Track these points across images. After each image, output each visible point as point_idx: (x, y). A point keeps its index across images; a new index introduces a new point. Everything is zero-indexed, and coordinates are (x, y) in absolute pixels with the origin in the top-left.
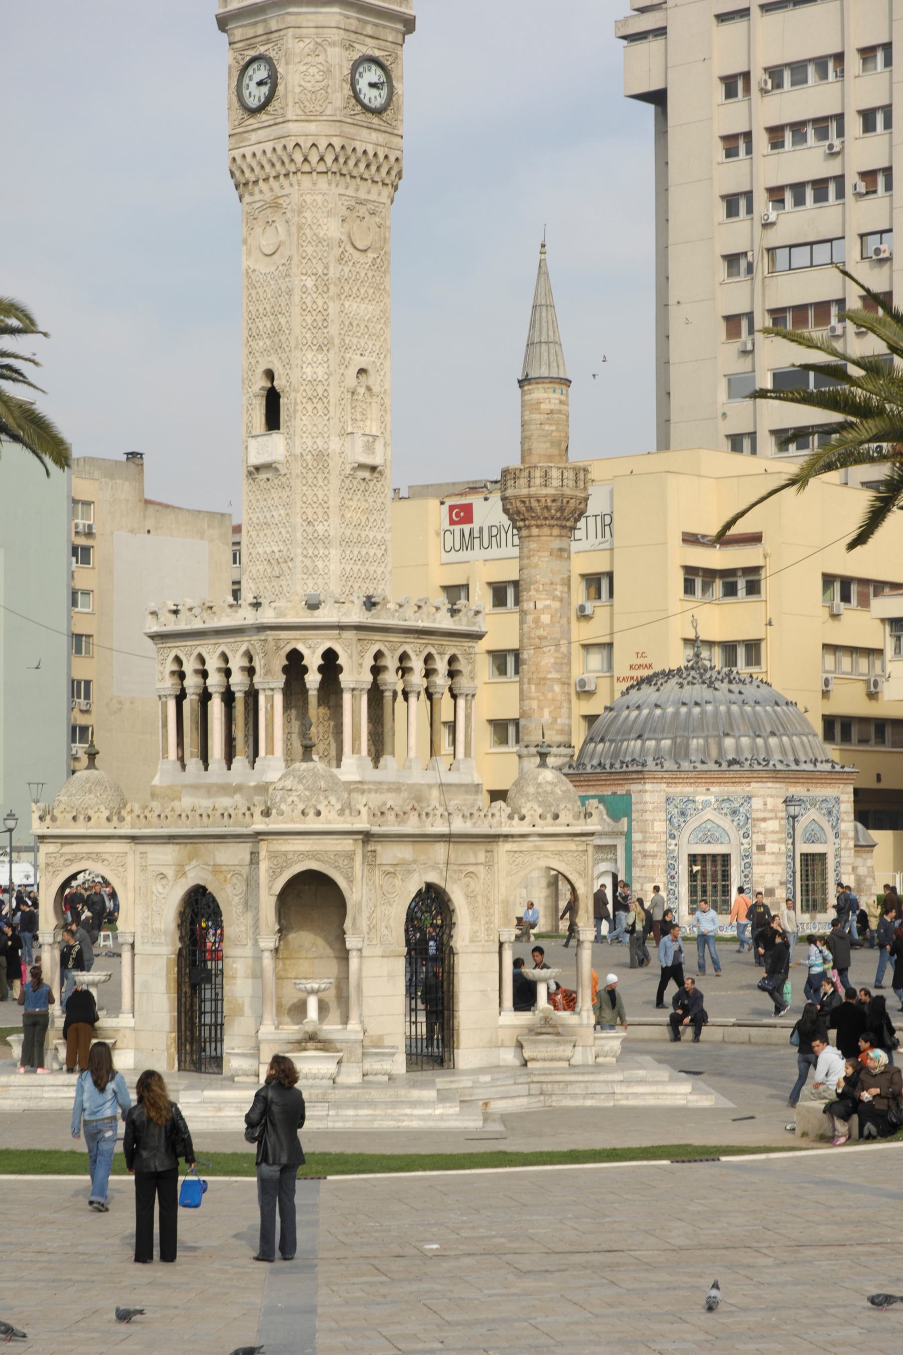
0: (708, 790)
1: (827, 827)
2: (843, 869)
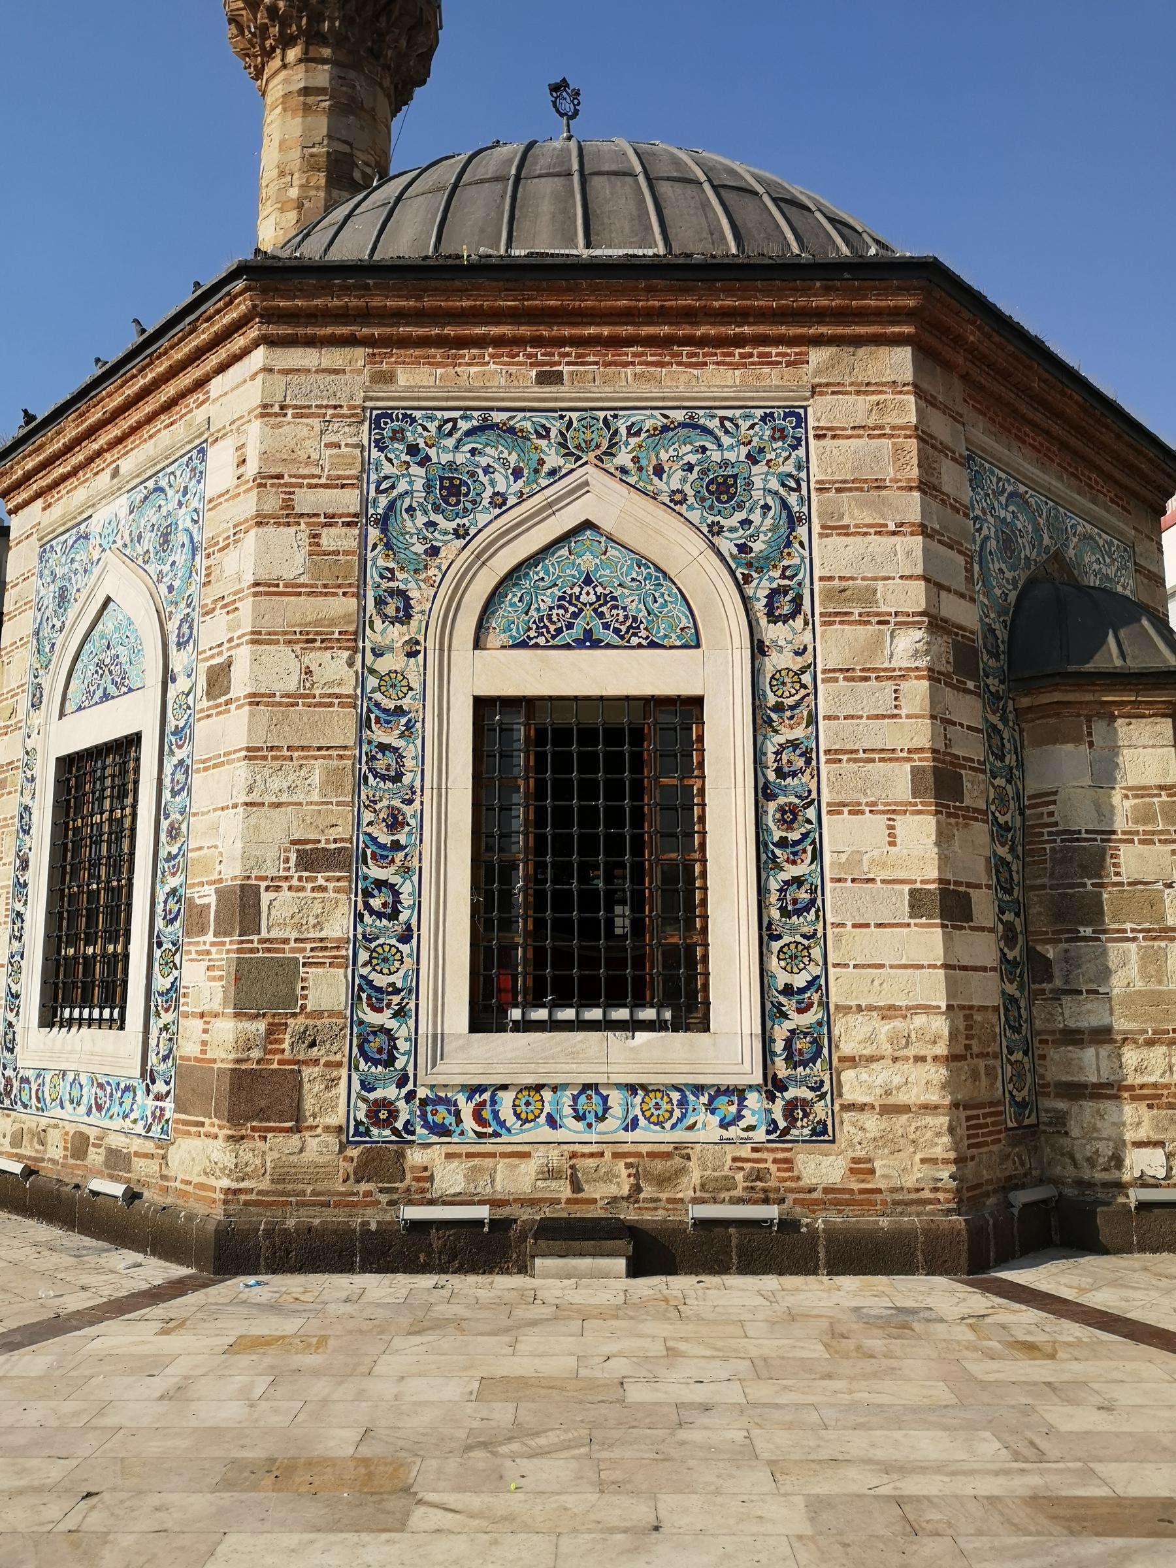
0: (115, 473)
2: (831, 782)
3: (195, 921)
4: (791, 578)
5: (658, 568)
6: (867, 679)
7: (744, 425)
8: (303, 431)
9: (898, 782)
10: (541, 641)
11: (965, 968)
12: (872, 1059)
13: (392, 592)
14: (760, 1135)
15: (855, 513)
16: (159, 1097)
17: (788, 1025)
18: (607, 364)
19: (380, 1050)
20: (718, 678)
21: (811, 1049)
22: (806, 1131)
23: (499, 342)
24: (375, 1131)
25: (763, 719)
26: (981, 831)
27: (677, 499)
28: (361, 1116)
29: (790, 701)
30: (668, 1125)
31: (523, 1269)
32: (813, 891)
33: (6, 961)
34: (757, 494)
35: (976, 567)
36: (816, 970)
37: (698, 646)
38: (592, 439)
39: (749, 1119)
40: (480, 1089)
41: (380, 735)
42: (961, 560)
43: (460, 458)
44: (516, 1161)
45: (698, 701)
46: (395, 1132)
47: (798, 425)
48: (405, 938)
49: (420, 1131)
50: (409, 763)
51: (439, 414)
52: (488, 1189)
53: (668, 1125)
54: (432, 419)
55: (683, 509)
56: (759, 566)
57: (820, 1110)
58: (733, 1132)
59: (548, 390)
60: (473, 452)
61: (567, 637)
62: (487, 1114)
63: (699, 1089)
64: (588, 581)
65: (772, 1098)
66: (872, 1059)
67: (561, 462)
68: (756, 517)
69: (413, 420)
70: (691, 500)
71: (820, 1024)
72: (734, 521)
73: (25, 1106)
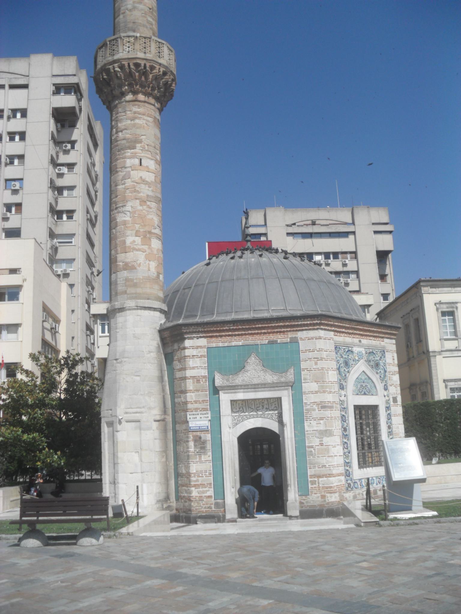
0: (360, 341)
1: (375, 378)
73: (356, 488)
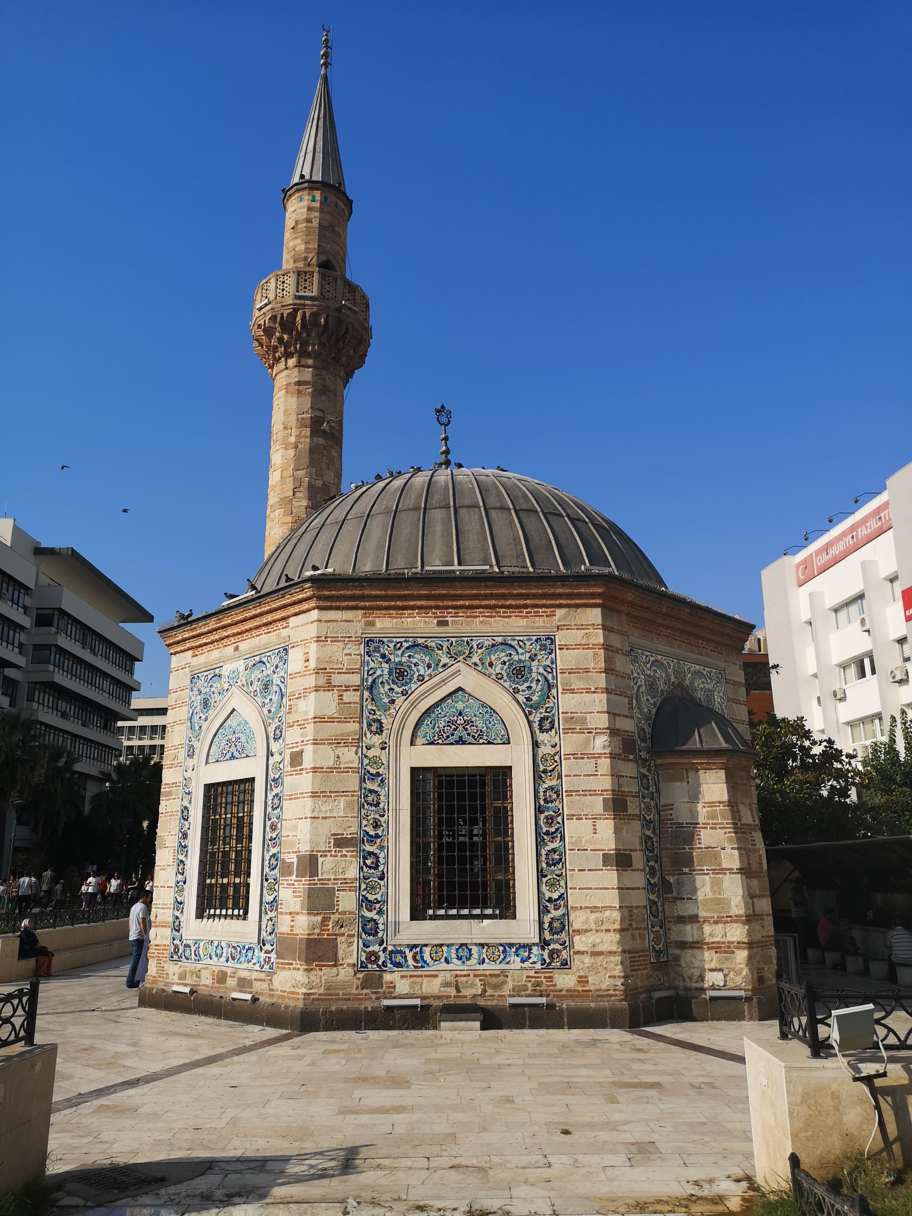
0: (237, 649)
2: (568, 805)
3: (287, 870)
4: (549, 712)
5: (491, 708)
6: (583, 758)
7: (528, 643)
8: (335, 648)
9: (597, 804)
10: (440, 741)
11: (629, 889)
12: (587, 931)
13: (374, 721)
14: (538, 966)
15: (577, 683)
16: (266, 952)
17: (550, 916)
18: (467, 617)
19: (371, 929)
20: (517, 758)
21: (560, 926)
22: (558, 964)
23: (420, 608)
24: (369, 966)
25: (538, 777)
26: (637, 825)
27: (499, 677)
28: (363, 959)
29: (550, 768)
30: (498, 962)
31: (435, 1028)
32: (560, 855)
33: (174, 885)
34: (534, 675)
35: (634, 701)
36: (562, 891)
37: (509, 743)
38: (461, 651)
39: (533, 959)
40: (416, 946)
41: (370, 785)
42: (626, 700)
43: (404, 660)
44: (431, 979)
45: (510, 768)
46: (378, 966)
47: (552, 644)
48: (381, 878)
49: (389, 965)
50: (382, 798)
51: (394, 640)
52: (419, 992)
53: (498, 962)
54: (392, 642)
55: (501, 681)
56: (536, 707)
57: (564, 954)
58: (526, 964)
59: (442, 629)
60: (409, 656)
61: (451, 739)
62: (418, 957)
63: (511, 945)
64: (460, 714)
65: (543, 949)
66: (587, 931)
67: (448, 661)
68: (534, 685)
69: (383, 643)
70: (505, 678)
71: (564, 915)
72: (524, 687)
73: (187, 959)
